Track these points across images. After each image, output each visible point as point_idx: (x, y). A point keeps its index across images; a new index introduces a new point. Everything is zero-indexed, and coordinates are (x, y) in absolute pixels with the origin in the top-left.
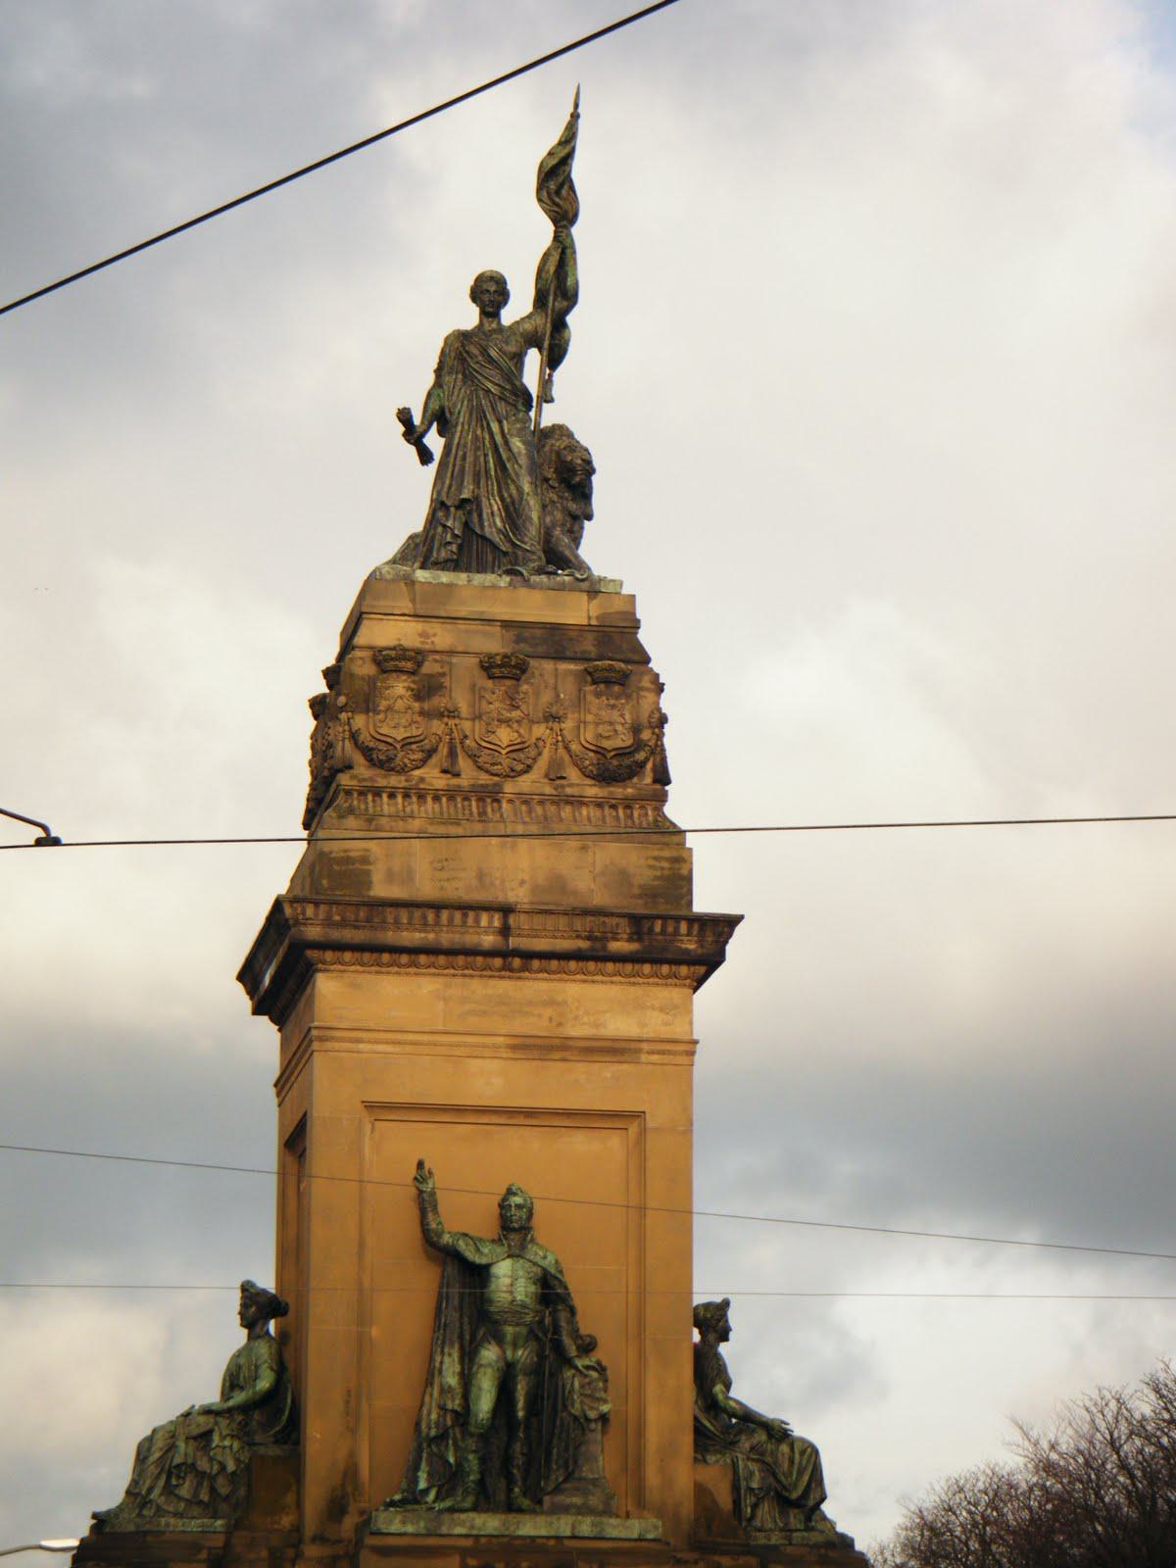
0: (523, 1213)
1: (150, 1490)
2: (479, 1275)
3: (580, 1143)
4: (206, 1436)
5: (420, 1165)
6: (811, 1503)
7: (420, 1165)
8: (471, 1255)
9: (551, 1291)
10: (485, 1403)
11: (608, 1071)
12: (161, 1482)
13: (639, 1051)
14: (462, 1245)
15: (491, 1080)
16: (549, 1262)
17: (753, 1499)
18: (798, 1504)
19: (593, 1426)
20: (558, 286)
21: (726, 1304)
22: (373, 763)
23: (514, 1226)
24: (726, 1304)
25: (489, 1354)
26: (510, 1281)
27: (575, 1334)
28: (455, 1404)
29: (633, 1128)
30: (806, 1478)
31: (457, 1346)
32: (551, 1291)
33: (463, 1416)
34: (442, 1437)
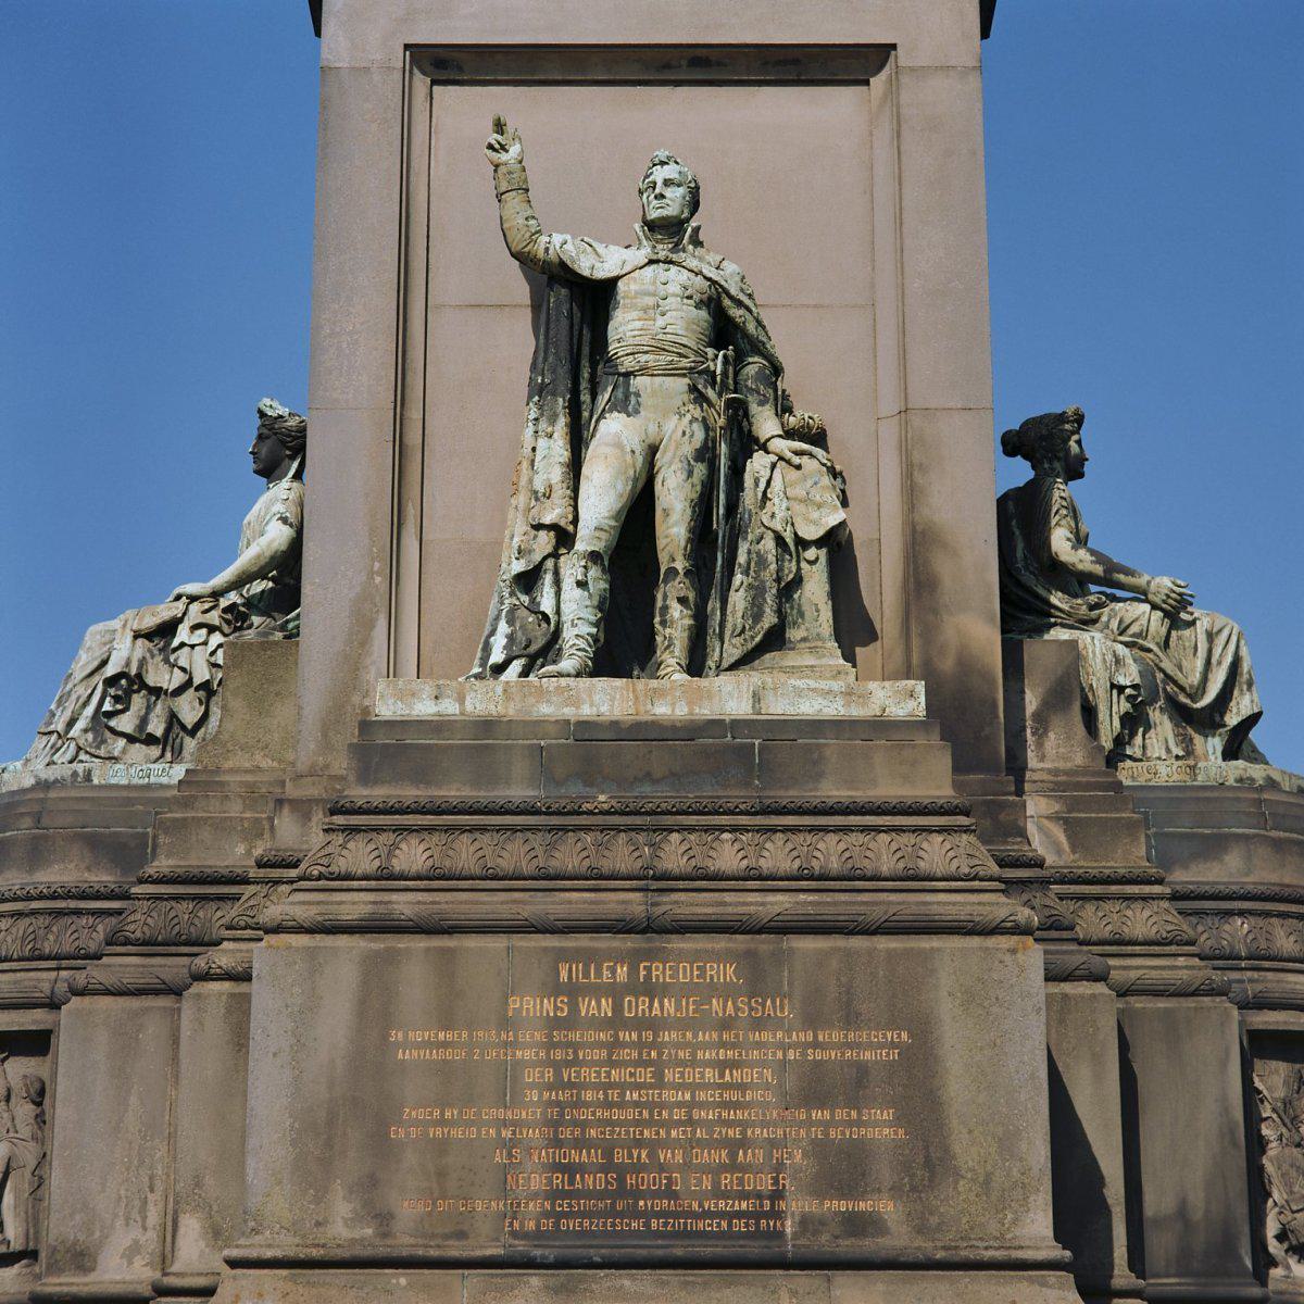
0: (676, 195)
1: (71, 723)
2: (597, 297)
4: (167, 629)
5: (499, 127)
6: (1232, 719)
10: (600, 503)
12: (90, 710)
16: (729, 275)
17: (1125, 706)
18: (1208, 720)
19: (811, 553)
25: (615, 433)
26: (653, 312)
31: (562, 421)
32: (726, 327)
34: (527, 581)
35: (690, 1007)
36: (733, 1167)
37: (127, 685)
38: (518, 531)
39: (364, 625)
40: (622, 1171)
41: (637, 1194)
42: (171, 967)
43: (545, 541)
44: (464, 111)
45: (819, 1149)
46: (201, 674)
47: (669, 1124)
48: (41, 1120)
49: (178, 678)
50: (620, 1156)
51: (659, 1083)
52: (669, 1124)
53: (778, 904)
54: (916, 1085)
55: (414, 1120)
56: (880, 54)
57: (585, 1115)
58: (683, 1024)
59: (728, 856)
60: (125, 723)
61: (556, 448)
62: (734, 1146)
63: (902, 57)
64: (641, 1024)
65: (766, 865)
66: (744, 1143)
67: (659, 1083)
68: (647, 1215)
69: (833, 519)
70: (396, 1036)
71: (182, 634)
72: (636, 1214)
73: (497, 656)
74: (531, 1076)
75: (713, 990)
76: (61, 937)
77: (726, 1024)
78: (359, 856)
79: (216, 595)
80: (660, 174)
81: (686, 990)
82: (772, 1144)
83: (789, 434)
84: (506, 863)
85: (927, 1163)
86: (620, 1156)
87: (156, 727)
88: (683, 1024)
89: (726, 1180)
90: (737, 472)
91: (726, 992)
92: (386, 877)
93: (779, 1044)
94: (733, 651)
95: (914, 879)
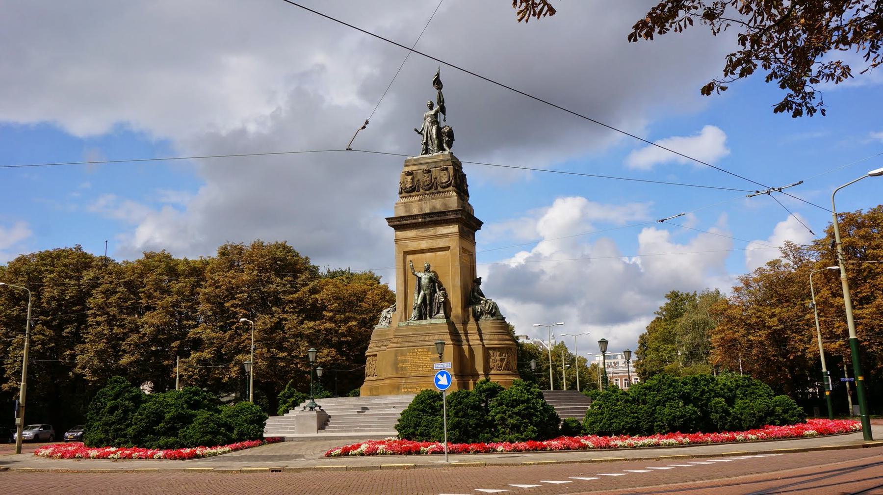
2: (420, 278)
15: (424, 245)
20: (441, 101)
44: (410, 257)
55: (400, 365)
56: (449, 247)
59: (427, 338)
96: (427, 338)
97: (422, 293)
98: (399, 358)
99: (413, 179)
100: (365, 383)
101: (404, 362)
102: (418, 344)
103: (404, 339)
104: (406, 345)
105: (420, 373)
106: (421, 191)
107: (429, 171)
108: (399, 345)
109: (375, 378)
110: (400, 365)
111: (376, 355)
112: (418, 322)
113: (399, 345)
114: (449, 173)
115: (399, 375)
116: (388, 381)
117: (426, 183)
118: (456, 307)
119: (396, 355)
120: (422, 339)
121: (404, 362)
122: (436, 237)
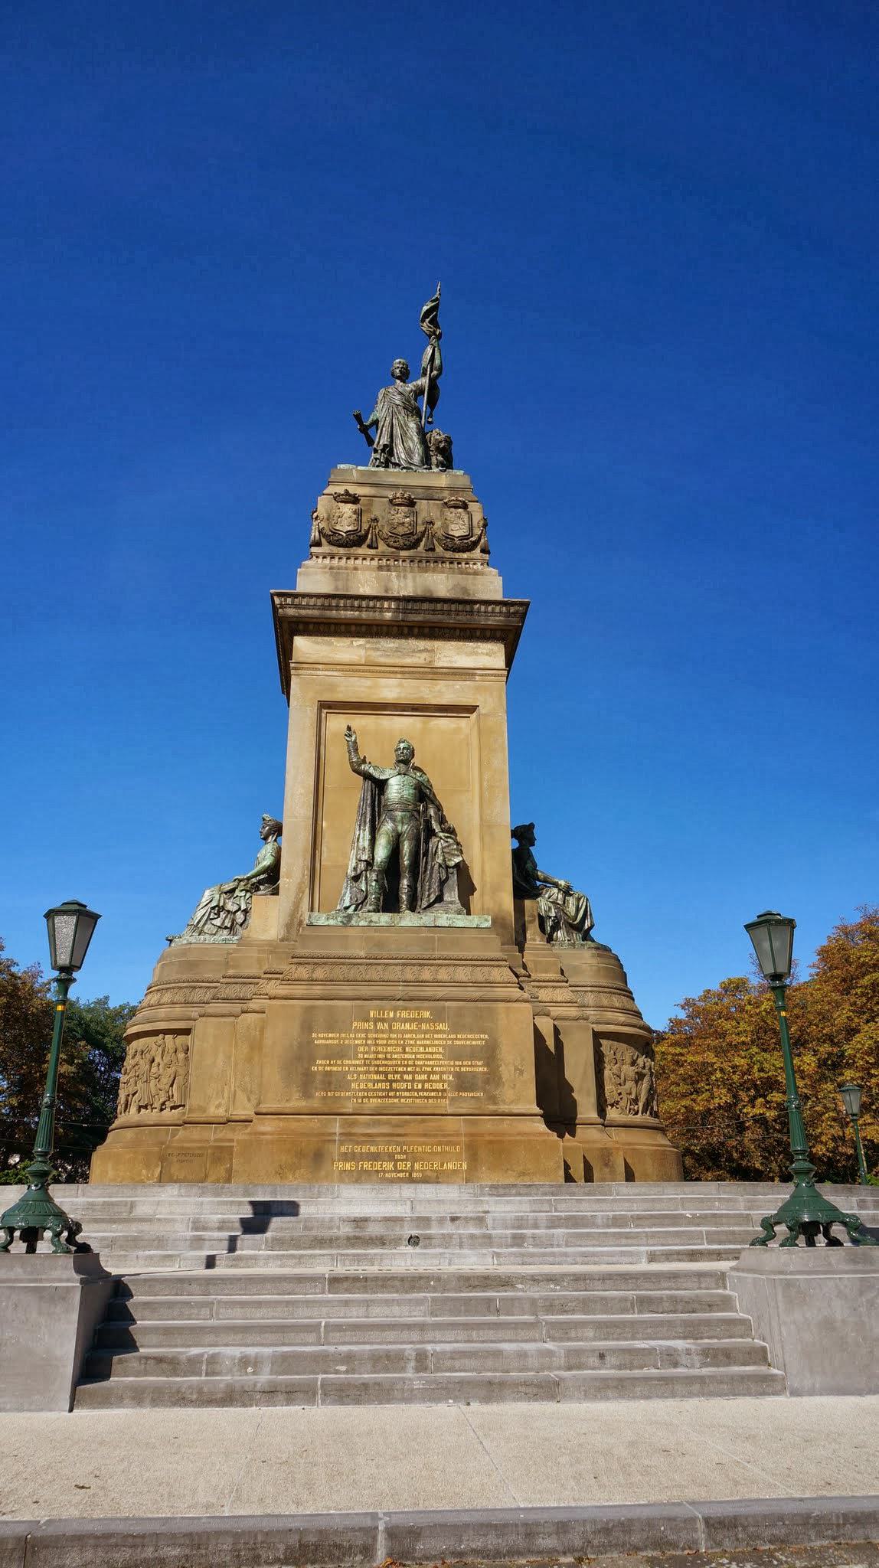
2: (381, 785)
3: (444, 723)
5: (349, 728)
7: (349, 728)
8: (376, 775)
9: (423, 794)
10: (381, 853)
11: (458, 685)
13: (474, 675)
14: (371, 771)
15: (390, 690)
21: (532, 826)
22: (330, 543)
23: (405, 760)
24: (532, 826)
27: (442, 820)
28: (365, 857)
29: (474, 716)
30: (581, 912)
32: (423, 794)
33: (369, 864)
34: (356, 878)
35: (414, 1027)
36: (429, 1081)
37: (219, 909)
38: (352, 863)
39: (300, 890)
40: (391, 1082)
41: (396, 1090)
42: (237, 1008)
43: (362, 866)
44: (336, 723)
45: (458, 1075)
46: (243, 907)
47: (407, 1066)
48: (187, 1059)
49: (235, 908)
50: (390, 1077)
51: (404, 1052)
52: (407, 1066)
53: (441, 992)
54: (490, 1054)
55: (320, 1066)
56: (471, 709)
57: (378, 1062)
58: (411, 1032)
59: (427, 974)
60: (218, 922)
61: (366, 835)
62: (429, 1074)
63: (482, 710)
64: (397, 1032)
65: (439, 977)
66: (433, 1073)
67: (404, 1052)
68: (400, 1097)
69: (457, 860)
70: (314, 1035)
71: (237, 893)
72: (395, 1097)
73: (347, 903)
74: (361, 1049)
75: (421, 1021)
76: (197, 995)
77: (426, 1032)
78: (303, 972)
79: (249, 879)
80: (402, 745)
81: (415, 1020)
82: (442, 1073)
83: (443, 831)
84: (351, 976)
85: (493, 1078)
86: (390, 1077)
87: (228, 923)
88: (411, 1032)
89: (427, 1086)
90: (427, 842)
91: (427, 1021)
92: (312, 981)
93: (442, 1037)
94: (425, 904)
95: (490, 983)
96: (427, 974)
97: (388, 827)
98: (321, 1039)
99: (359, 514)
100: (110, 1136)
101: (339, 1053)
102: (400, 990)
103: (338, 972)
104: (348, 990)
105: (406, 1102)
106: (382, 547)
107: (411, 503)
108: (317, 990)
109: (168, 1115)
110: (320, 1066)
111: (187, 1032)
112: (384, 918)
113: (317, 990)
114: (471, 519)
115: (315, 1104)
116: (268, 1126)
117: (401, 530)
118: (496, 889)
119: (307, 1027)
120: (409, 974)
121: (339, 1053)
122: (433, 673)
